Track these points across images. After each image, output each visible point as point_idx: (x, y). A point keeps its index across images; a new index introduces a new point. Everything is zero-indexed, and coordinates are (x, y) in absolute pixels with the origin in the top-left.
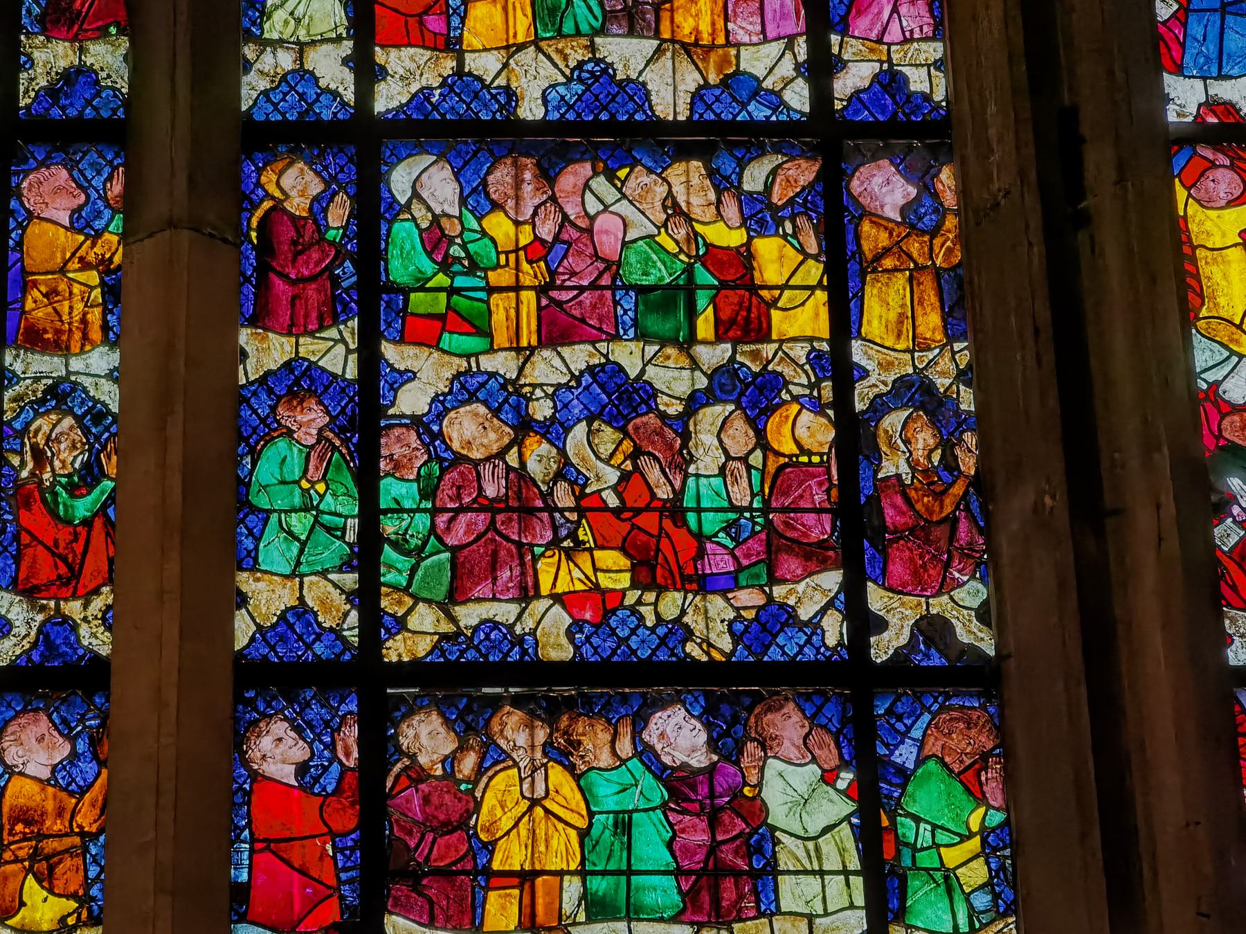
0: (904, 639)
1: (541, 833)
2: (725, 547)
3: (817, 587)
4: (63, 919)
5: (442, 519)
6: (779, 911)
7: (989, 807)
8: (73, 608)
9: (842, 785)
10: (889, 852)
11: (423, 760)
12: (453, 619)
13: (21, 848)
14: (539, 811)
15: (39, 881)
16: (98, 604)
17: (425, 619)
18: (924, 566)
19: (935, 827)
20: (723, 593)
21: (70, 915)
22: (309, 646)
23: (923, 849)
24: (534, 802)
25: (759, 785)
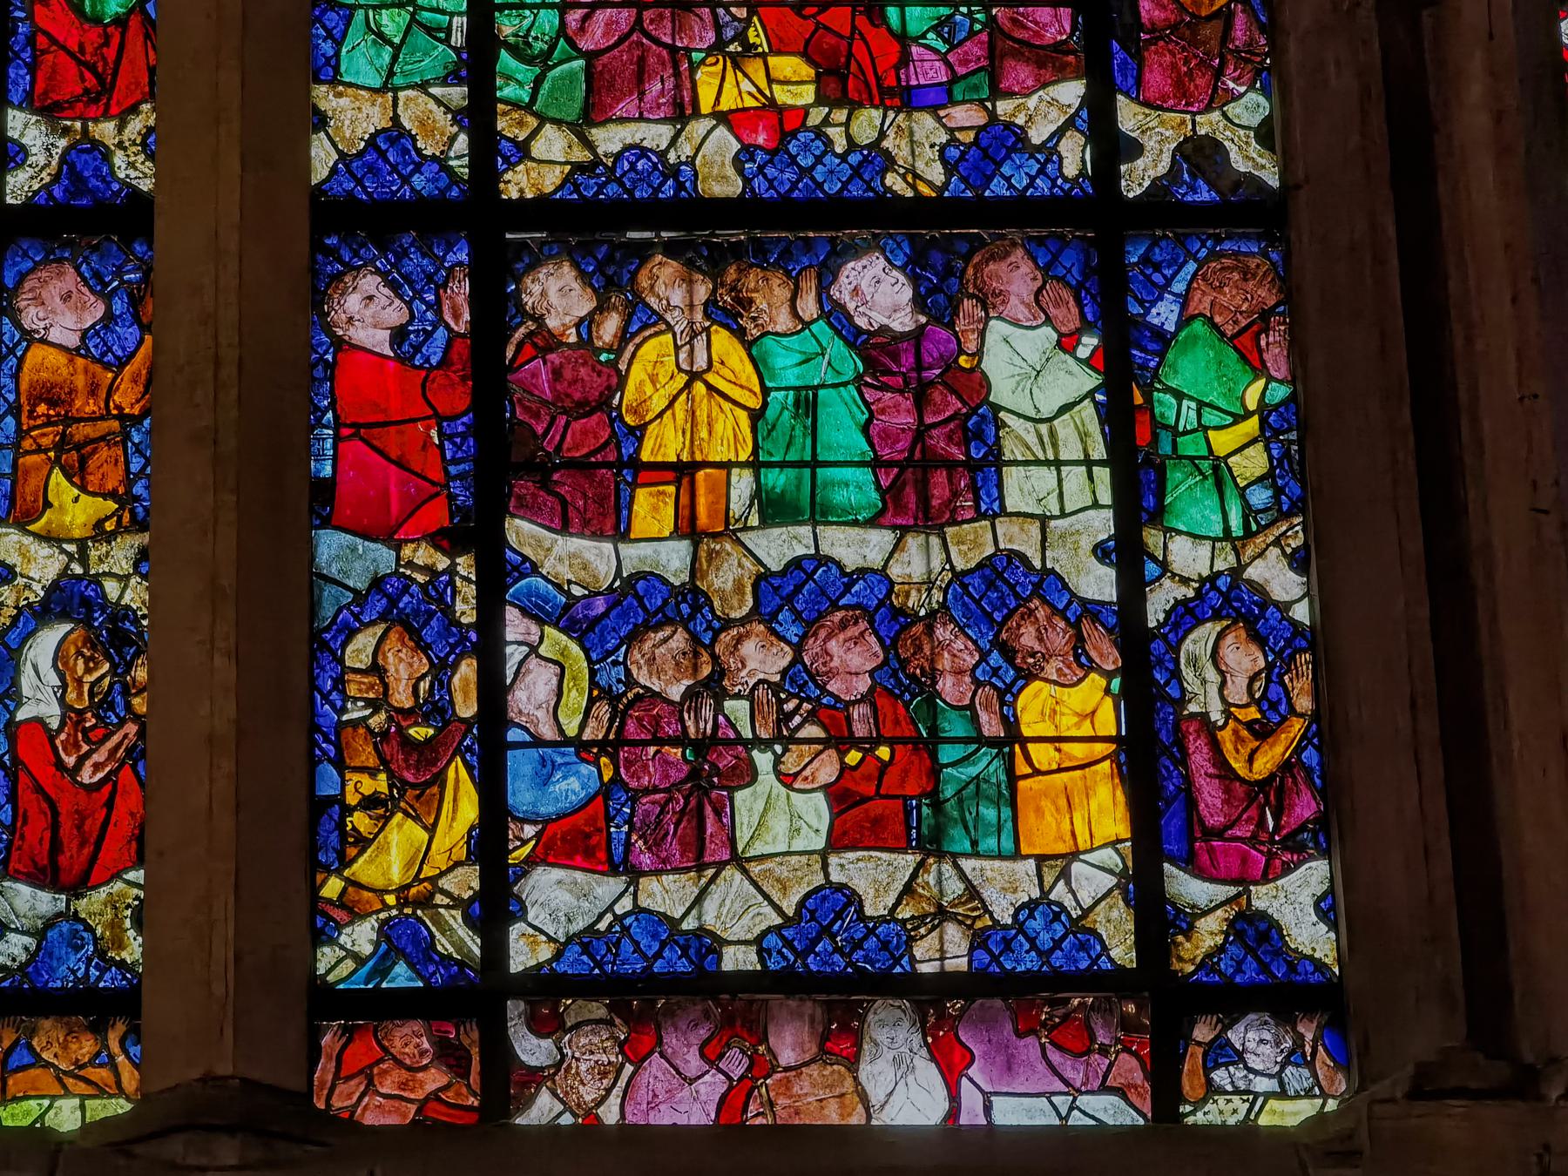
0: (1164, 166)
1: (702, 415)
2: (936, 51)
3: (1053, 102)
4: (99, 524)
5: (574, 16)
6: (1003, 511)
7: (1270, 379)
8: (105, 130)
9: (1084, 352)
10: (1142, 436)
11: (552, 323)
12: (589, 145)
13: (44, 435)
14: (699, 388)
15: (69, 477)
16: (135, 126)
17: (553, 145)
18: (1190, 72)
19: (1201, 405)
20: (933, 109)
21: (108, 518)
22: (406, 180)
23: (1186, 433)
24: (694, 376)
25: (979, 353)
